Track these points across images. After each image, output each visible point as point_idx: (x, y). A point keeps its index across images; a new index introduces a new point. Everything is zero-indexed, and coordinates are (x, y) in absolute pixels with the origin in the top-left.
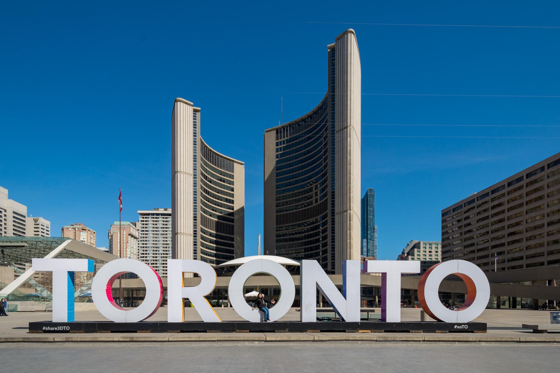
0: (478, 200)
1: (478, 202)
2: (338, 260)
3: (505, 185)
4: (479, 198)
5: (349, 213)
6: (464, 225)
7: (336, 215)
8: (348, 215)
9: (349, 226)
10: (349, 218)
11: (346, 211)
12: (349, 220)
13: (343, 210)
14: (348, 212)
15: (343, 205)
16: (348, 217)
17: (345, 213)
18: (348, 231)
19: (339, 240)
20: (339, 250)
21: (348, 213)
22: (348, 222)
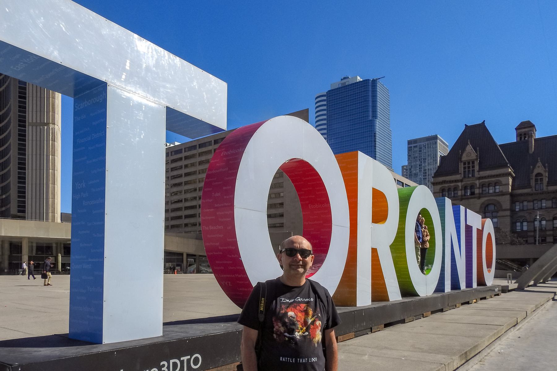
0: (185, 151)
1: (186, 153)
2: (32, 198)
3: (211, 141)
4: (187, 149)
5: (52, 128)
6: (171, 177)
7: (28, 126)
8: (51, 132)
9: (52, 149)
10: (52, 137)
11: (48, 124)
12: (52, 138)
13: (42, 121)
14: (51, 126)
15: (42, 113)
16: (51, 134)
17: (45, 127)
18: (50, 156)
19: (34, 168)
20: (34, 183)
21: (51, 128)
22: (51, 142)
